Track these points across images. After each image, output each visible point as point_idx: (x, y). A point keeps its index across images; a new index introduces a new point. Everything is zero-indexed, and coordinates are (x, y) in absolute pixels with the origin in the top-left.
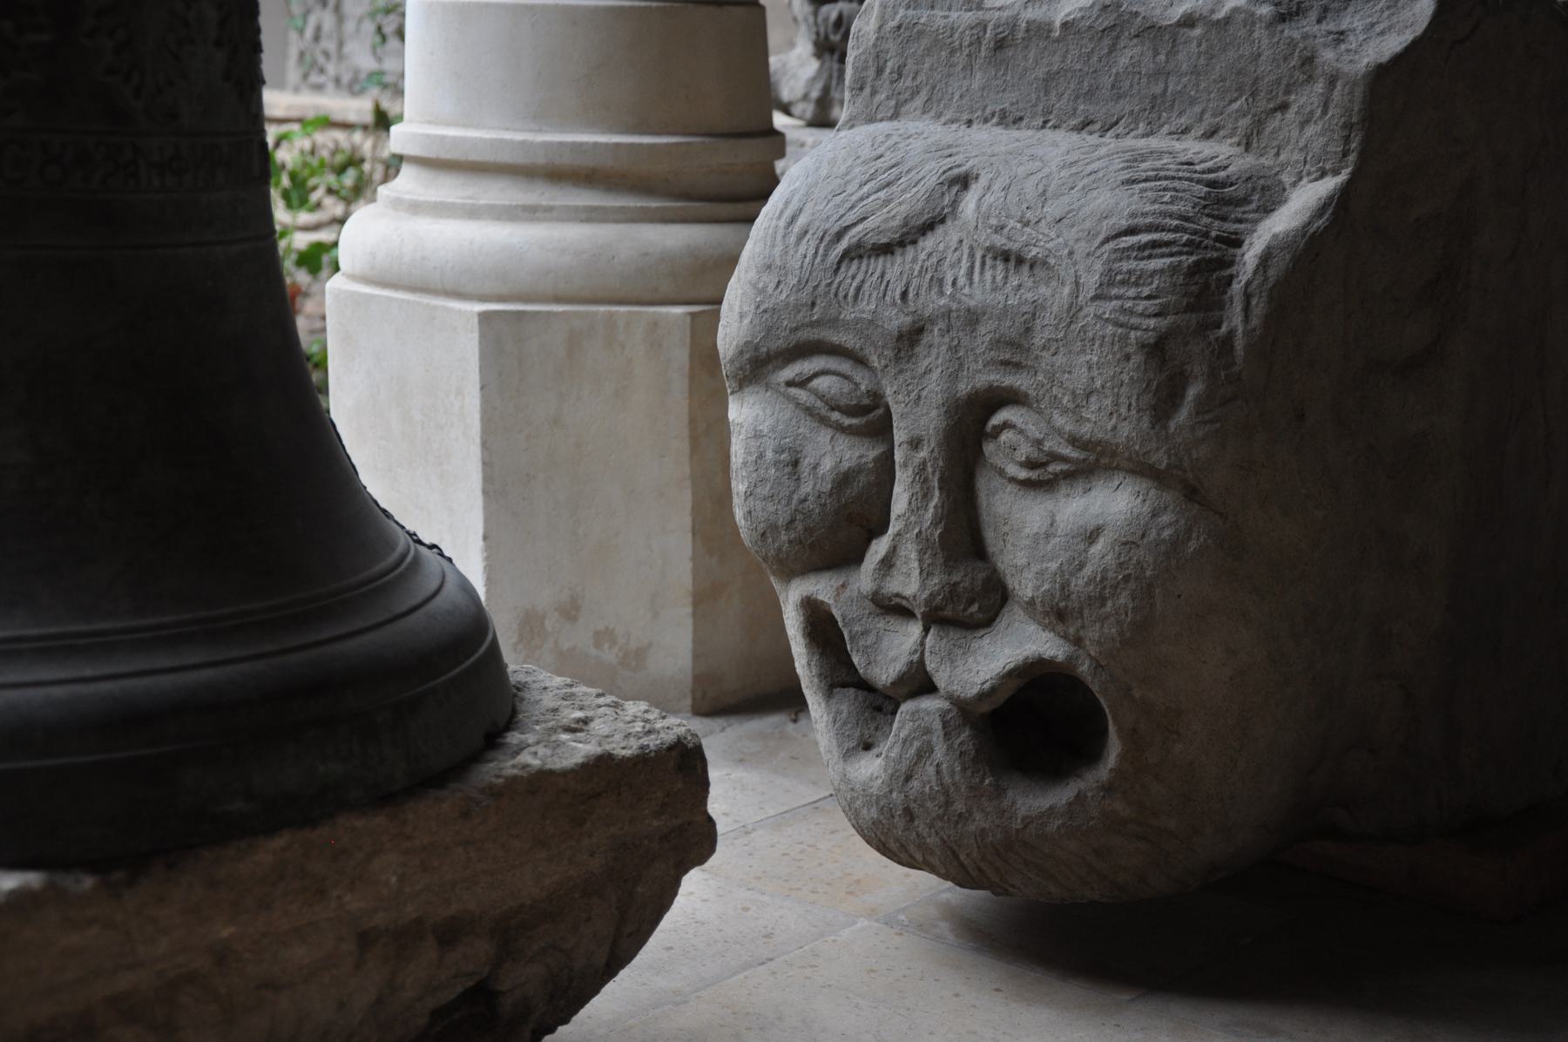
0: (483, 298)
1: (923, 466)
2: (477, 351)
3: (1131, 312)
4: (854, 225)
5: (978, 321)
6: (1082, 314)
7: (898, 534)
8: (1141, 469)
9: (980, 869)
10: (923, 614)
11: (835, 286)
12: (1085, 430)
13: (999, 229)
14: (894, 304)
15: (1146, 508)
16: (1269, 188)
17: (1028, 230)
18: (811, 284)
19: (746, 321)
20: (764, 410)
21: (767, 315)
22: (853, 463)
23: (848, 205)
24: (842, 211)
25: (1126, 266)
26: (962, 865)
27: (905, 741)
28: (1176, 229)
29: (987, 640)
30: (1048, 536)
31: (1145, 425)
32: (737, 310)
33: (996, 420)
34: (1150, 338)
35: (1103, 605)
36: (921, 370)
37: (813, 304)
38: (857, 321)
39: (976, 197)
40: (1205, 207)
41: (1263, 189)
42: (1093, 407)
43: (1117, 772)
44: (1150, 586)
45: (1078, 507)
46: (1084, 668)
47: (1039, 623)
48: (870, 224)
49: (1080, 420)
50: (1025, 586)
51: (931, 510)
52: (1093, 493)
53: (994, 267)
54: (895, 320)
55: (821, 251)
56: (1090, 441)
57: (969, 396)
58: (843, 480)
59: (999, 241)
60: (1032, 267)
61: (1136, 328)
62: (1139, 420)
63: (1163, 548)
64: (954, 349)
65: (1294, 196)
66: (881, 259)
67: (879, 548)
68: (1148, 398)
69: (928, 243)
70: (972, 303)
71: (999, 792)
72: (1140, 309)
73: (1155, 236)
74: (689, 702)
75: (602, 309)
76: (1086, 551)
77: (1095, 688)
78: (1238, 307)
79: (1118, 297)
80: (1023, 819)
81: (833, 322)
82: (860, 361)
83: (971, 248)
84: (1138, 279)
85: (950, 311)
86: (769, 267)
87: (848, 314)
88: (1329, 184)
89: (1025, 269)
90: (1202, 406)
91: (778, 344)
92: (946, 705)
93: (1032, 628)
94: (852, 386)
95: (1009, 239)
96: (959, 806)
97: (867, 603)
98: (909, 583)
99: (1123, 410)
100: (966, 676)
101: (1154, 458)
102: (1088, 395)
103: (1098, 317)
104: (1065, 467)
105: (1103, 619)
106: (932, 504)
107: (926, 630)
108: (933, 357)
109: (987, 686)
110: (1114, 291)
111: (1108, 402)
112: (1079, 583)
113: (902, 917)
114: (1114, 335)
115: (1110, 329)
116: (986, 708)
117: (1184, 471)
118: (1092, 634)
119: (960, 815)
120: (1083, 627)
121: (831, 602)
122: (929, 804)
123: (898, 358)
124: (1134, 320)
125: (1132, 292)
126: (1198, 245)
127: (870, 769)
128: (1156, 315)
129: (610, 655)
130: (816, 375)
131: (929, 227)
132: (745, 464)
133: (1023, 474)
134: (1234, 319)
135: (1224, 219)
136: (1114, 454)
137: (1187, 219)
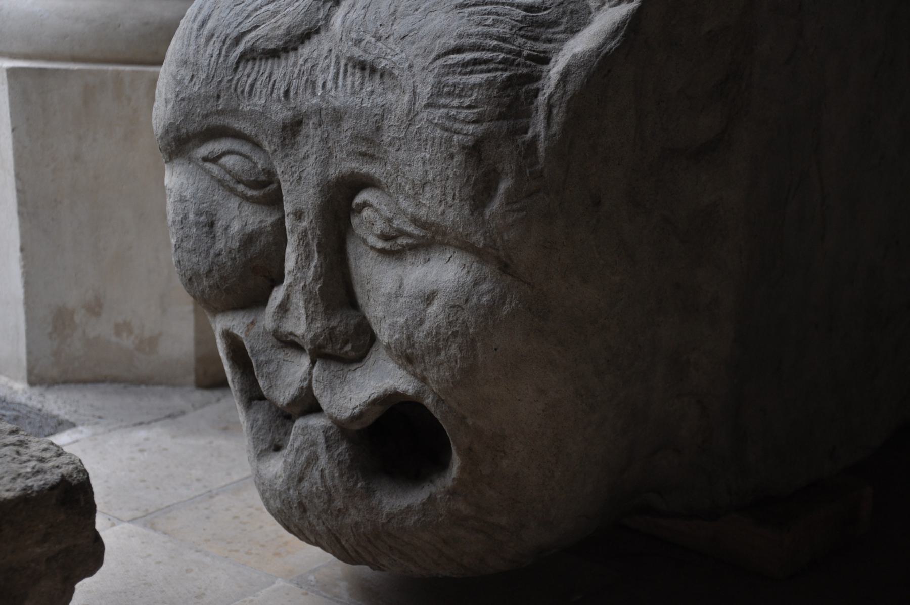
0: (13, 56)
1: (305, 233)
2: (6, 99)
3: (455, 119)
4: (249, 31)
5: (341, 119)
6: (417, 118)
7: (290, 286)
8: (466, 247)
9: (357, 552)
10: (310, 350)
11: (234, 82)
12: (423, 212)
13: (358, 42)
14: (279, 100)
15: (469, 279)
16: (577, 12)
17: (379, 44)
18: (217, 80)
19: (170, 106)
20: (188, 179)
21: (184, 102)
22: (256, 227)
23: (245, 14)
24: (240, 19)
25: (452, 80)
26: (343, 547)
27: (297, 450)
28: (494, 49)
29: (358, 373)
30: (398, 296)
31: (466, 212)
32: (164, 96)
33: (359, 199)
34: (469, 141)
35: (439, 354)
36: (301, 156)
37: (219, 97)
38: (252, 112)
39: (343, 14)
40: (520, 29)
41: (572, 12)
42: (428, 195)
43: (459, 480)
44: (473, 341)
46: (428, 401)
47: (396, 363)
48: (260, 32)
49: (419, 205)
50: (384, 334)
51: (313, 269)
52: (431, 263)
53: (353, 74)
54: (281, 114)
55: (224, 52)
56: (426, 222)
57: (337, 178)
58: (249, 240)
59: (357, 52)
60: (382, 76)
61: (458, 133)
62: (461, 208)
63: (482, 311)
64: (325, 140)
65: (596, 19)
66: (270, 62)
67: (278, 295)
68: (467, 190)
69: (305, 50)
70: (337, 104)
71: (369, 492)
72: (462, 116)
73: (477, 55)
74: (192, 378)
75: (111, 68)
76: (424, 310)
77: (438, 417)
78: (542, 115)
79: (445, 106)
80: (388, 515)
81: (234, 112)
82: (257, 145)
83: (337, 57)
84: (459, 91)
85: (321, 109)
86: (185, 62)
87: (245, 106)
88: (625, 9)
89: (377, 77)
90: (511, 198)
91: (193, 127)
92: (328, 423)
93: (391, 365)
94: (251, 165)
95: (365, 51)
96: (338, 504)
97: (271, 338)
98: (298, 325)
99: (449, 199)
100: (341, 401)
101: (474, 239)
102: (424, 185)
103: (430, 122)
104: (410, 241)
105: (439, 365)
106: (313, 264)
107: (313, 363)
108: (310, 144)
109: (357, 411)
110: (442, 101)
111: (438, 191)
112: (419, 336)
113: (312, 577)
114: (441, 137)
115: (438, 132)
116: (357, 427)
117: (498, 250)
118: (432, 375)
119: (339, 510)
120: (425, 369)
121: (243, 336)
122: (316, 501)
123: (283, 145)
124: (457, 126)
125: (456, 102)
126: (512, 63)
127: (276, 466)
128: (474, 122)
129: (128, 342)
130: (224, 154)
131: (306, 37)
132: (174, 222)
133: (380, 244)
134: (538, 125)
135: (536, 39)
136: (445, 234)
137: (504, 40)
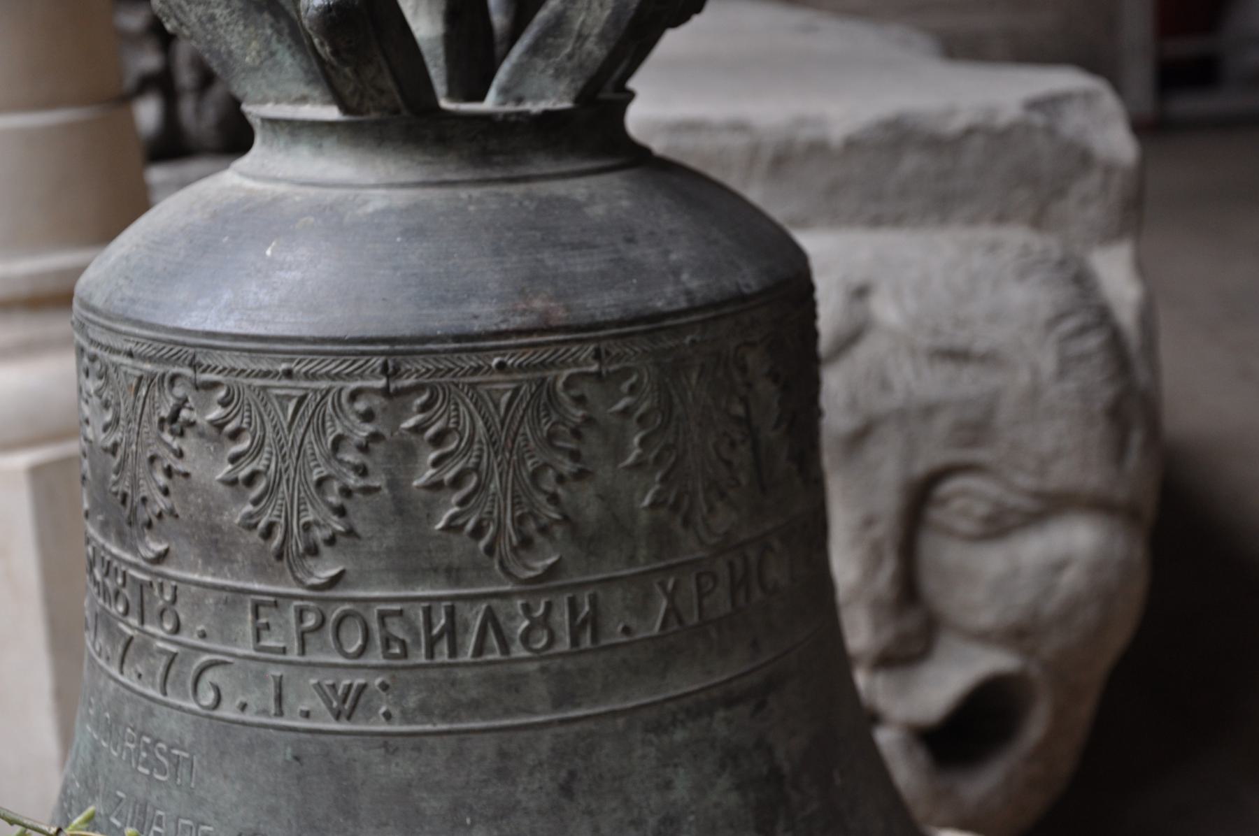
8: (1098, 505)
45: (1035, 548)
112: (1051, 607)
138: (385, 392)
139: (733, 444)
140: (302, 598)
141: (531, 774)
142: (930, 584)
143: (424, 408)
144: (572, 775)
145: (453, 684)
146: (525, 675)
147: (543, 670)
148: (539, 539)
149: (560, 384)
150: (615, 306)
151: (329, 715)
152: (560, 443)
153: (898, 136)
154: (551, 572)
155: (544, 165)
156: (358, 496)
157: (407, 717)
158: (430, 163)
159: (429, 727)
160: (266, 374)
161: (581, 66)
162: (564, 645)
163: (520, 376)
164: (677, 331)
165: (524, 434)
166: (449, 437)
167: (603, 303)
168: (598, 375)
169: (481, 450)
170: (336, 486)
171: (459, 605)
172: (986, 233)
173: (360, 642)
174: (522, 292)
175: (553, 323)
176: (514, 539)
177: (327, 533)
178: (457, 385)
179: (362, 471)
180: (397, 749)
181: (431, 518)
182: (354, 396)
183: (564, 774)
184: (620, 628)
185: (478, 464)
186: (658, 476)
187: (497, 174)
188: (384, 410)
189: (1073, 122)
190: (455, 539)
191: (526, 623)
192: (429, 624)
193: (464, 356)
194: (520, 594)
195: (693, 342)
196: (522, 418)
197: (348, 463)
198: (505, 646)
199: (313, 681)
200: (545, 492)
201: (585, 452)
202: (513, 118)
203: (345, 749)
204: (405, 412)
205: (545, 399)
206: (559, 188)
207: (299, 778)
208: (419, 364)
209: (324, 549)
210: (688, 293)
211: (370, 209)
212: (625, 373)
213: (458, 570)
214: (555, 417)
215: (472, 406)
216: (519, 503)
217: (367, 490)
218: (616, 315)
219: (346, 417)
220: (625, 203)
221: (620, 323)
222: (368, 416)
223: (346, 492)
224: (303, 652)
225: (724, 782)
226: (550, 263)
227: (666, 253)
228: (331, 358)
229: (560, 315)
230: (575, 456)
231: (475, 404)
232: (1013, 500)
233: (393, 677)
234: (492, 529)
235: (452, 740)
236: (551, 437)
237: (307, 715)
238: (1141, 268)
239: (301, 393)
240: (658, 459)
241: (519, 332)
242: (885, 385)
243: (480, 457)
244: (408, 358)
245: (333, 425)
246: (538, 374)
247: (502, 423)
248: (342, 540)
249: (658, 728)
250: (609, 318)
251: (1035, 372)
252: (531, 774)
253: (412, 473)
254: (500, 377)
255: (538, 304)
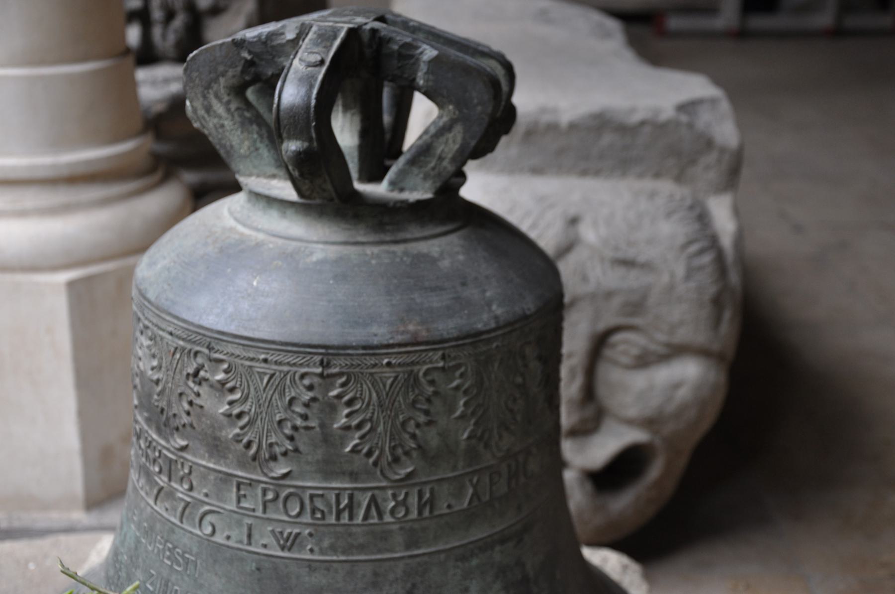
8: (702, 352)
112: (671, 408)
138: (321, 375)
139: (515, 400)
140: (266, 483)
141: (391, 585)
142: (602, 391)
143: (343, 385)
144: (414, 586)
145: (350, 535)
146: (391, 531)
147: (401, 529)
148: (403, 458)
149: (421, 374)
150: (455, 328)
151: (278, 548)
152: (419, 406)
153: (601, 123)
154: (409, 476)
155: (415, 231)
156: (302, 431)
157: (322, 552)
158: (349, 229)
159: (335, 558)
160: (252, 359)
161: (439, 174)
162: (414, 515)
163: (399, 369)
164: (489, 341)
165: (399, 401)
166: (356, 402)
167: (448, 327)
168: (443, 369)
169: (374, 410)
170: (289, 424)
171: (356, 493)
172: (648, 184)
173: (298, 510)
174: (402, 320)
175: (419, 339)
176: (390, 459)
177: (283, 449)
178: (362, 373)
179: (305, 417)
180: (315, 570)
181: (343, 445)
182: (303, 376)
183: (409, 585)
184: (445, 505)
185: (371, 418)
186: (473, 422)
187: (388, 238)
188: (320, 385)
189: (704, 118)
190: (356, 457)
191: (393, 504)
192: (338, 502)
193: (368, 358)
194: (391, 488)
195: (497, 347)
196: (398, 392)
197: (297, 413)
198: (380, 515)
199: (270, 528)
200: (409, 433)
201: (432, 410)
202: (398, 205)
203: (287, 567)
204: (332, 386)
205: (412, 381)
206: (422, 247)
207: (259, 580)
208: (342, 361)
209: (280, 457)
210: (496, 318)
211: (314, 258)
212: (458, 366)
213: (357, 474)
214: (417, 392)
215: (370, 385)
216: (394, 439)
217: (307, 428)
218: (455, 334)
219: (298, 387)
220: (461, 257)
221: (457, 339)
222: (310, 388)
223: (295, 428)
224: (265, 511)
225: (497, 586)
226: (418, 301)
227: (484, 291)
228: (290, 354)
229: (424, 335)
230: (427, 413)
231: (372, 384)
232: (653, 347)
233: (316, 530)
234: (377, 453)
235: (347, 566)
236: (414, 402)
237: (265, 546)
238: (737, 211)
239: (272, 372)
240: (473, 413)
241: (400, 345)
242: (585, 279)
243: (373, 413)
244: (336, 357)
245: (290, 391)
246: (409, 368)
247: (387, 395)
248: (290, 454)
249: (463, 558)
250: (451, 336)
251: (672, 275)
252: (391, 585)
253: (333, 420)
254: (387, 369)
255: (411, 327)
